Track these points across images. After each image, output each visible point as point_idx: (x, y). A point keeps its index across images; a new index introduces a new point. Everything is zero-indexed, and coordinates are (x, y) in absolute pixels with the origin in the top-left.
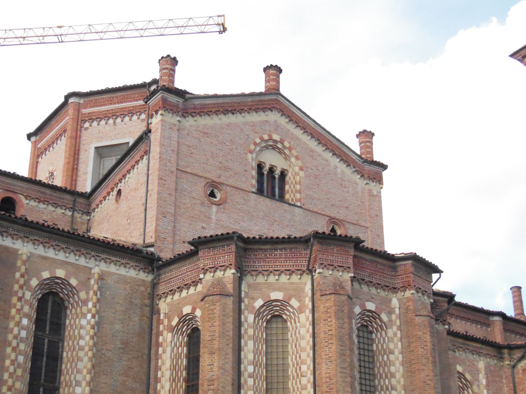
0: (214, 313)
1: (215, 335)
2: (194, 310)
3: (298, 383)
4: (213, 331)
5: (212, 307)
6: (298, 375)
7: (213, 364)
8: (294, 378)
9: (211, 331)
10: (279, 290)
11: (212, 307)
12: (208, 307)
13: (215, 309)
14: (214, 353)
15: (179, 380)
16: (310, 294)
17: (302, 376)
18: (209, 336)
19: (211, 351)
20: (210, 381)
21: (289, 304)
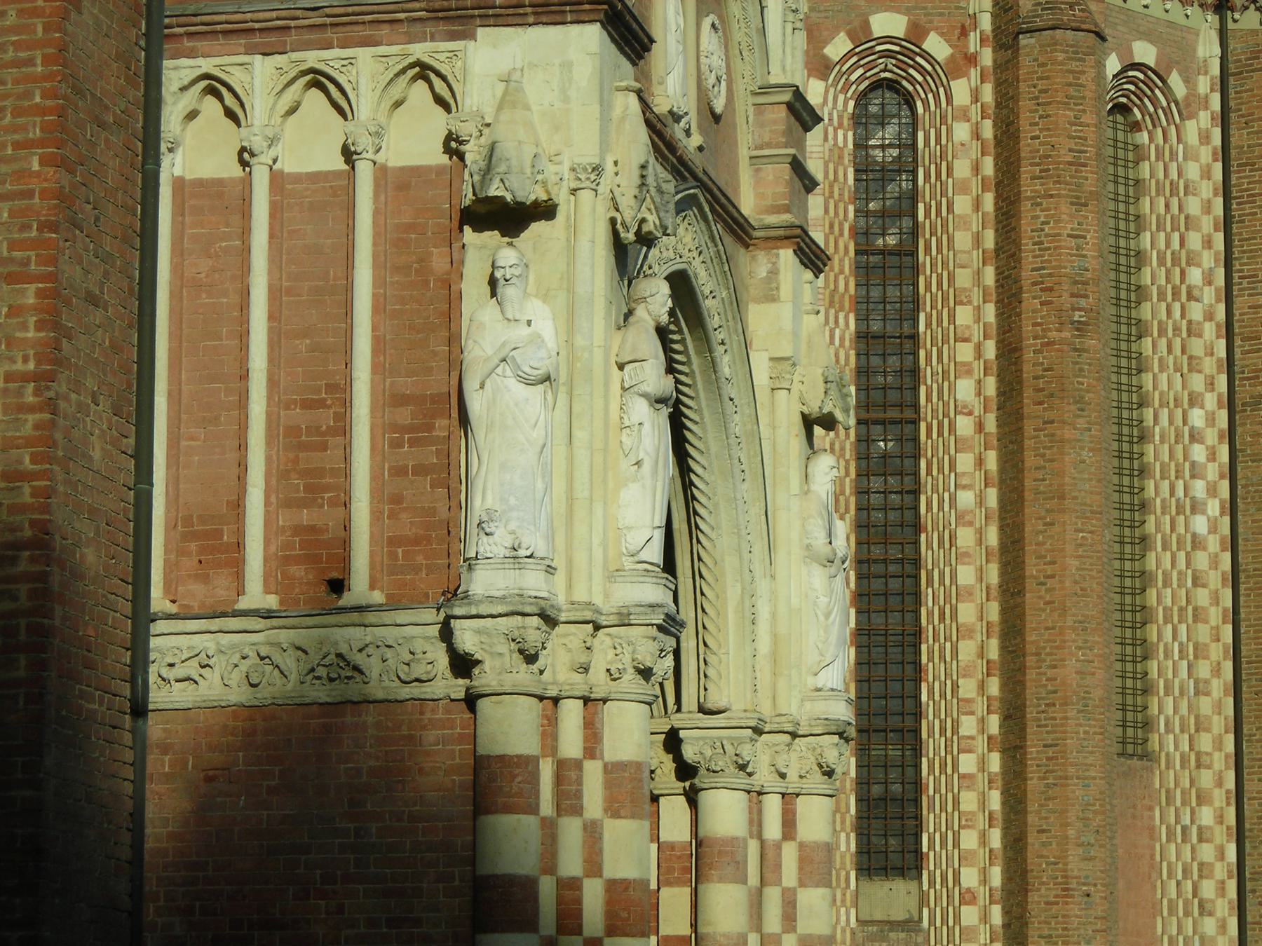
0: (1081, 85)
1: (1085, 152)
2: (916, 33)
3: (1177, 314)
4: (1080, 138)
5: (1074, 63)
6: (1176, 293)
7: (1085, 237)
8: (1162, 296)
9: (1074, 138)
10: (1148, 36)
11: (1074, 65)
12: (1062, 64)
13: (1083, 72)
14: (1086, 205)
15: (841, 234)
16: (1216, 70)
17: (1190, 297)
18: (1070, 150)
19: (1078, 198)
20: (1076, 283)
21: (1163, 81)
